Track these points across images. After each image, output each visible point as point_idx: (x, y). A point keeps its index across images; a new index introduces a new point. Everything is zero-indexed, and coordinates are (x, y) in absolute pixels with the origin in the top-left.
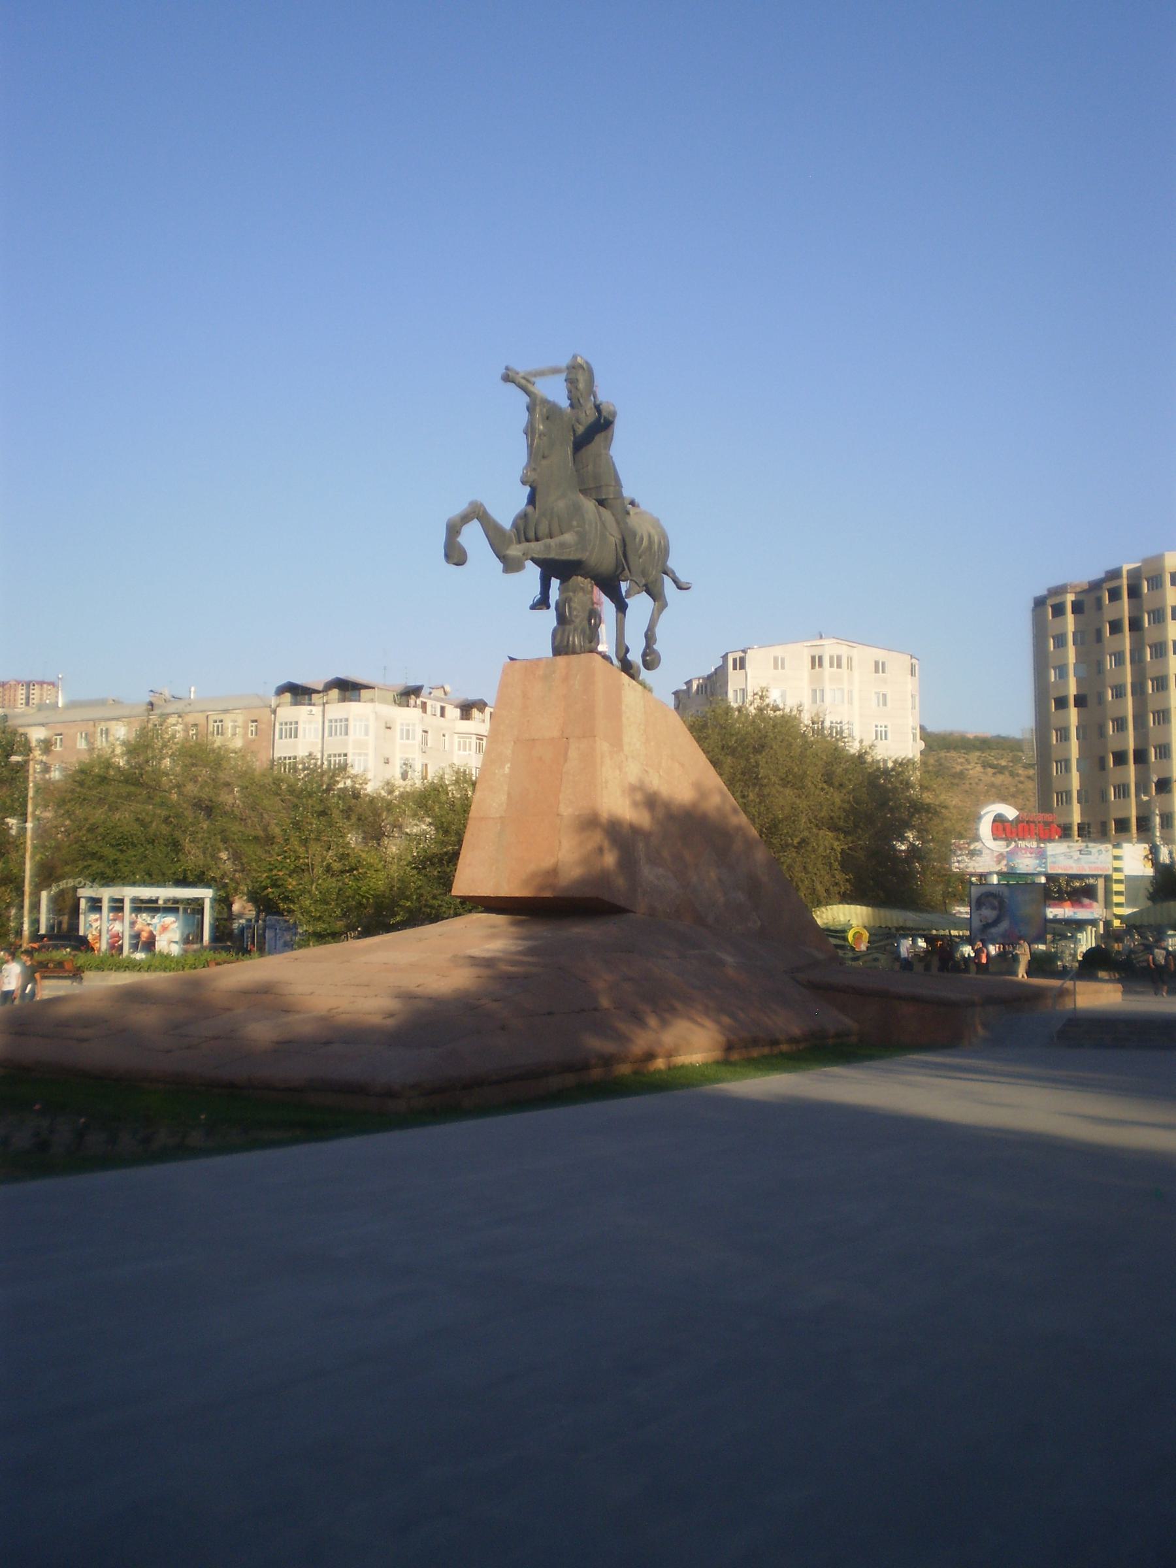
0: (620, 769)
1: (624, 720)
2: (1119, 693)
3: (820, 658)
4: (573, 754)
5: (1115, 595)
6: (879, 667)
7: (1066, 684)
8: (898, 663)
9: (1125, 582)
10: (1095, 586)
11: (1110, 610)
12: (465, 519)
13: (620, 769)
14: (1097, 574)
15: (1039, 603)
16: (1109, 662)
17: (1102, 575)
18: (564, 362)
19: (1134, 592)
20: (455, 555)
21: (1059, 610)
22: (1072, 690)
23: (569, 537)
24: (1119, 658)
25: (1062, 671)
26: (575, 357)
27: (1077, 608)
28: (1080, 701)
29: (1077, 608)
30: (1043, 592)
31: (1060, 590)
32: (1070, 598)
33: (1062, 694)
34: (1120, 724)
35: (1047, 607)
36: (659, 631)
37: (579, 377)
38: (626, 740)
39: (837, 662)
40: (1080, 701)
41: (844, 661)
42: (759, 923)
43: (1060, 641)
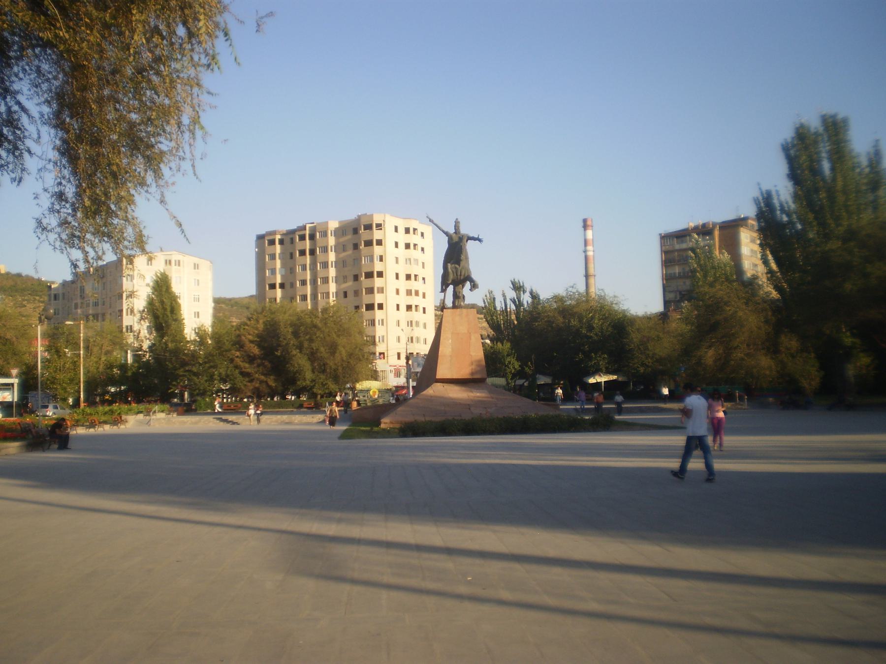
2: (304, 283)
3: (170, 261)
4: (473, 337)
5: (302, 238)
6: (196, 266)
7: (275, 278)
8: (205, 265)
9: (307, 232)
10: (293, 232)
11: (299, 245)
14: (293, 227)
15: (260, 238)
16: (298, 269)
17: (294, 227)
19: (312, 237)
21: (272, 242)
22: (279, 280)
24: (304, 268)
25: (273, 271)
27: (281, 242)
28: (282, 286)
29: (281, 242)
30: (263, 232)
31: (274, 233)
32: (278, 237)
33: (273, 282)
34: (304, 298)
35: (264, 241)
39: (178, 263)
40: (282, 286)
41: (181, 263)
43: (273, 257)
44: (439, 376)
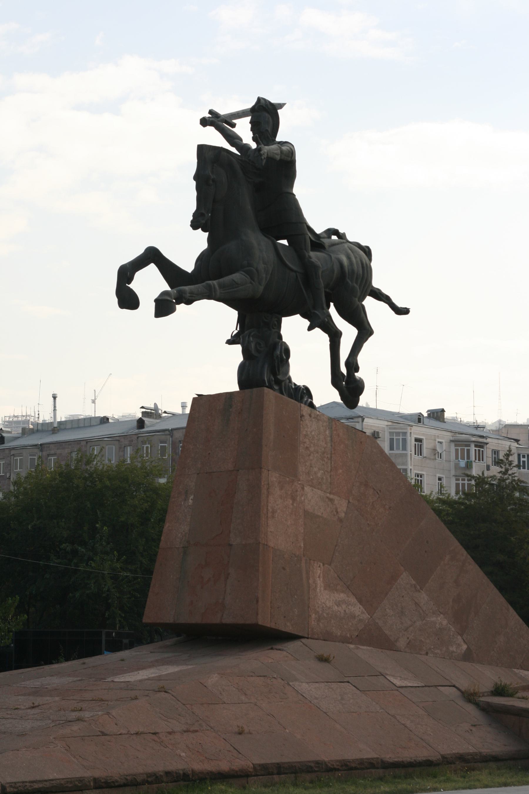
0: (294, 499)
1: (301, 450)
12: (139, 263)
13: (294, 499)
18: (250, 104)
20: (128, 300)
23: (237, 277)
26: (259, 99)
36: (361, 359)
37: (265, 115)
38: (301, 469)
42: (465, 647)
44: (150, 616)
